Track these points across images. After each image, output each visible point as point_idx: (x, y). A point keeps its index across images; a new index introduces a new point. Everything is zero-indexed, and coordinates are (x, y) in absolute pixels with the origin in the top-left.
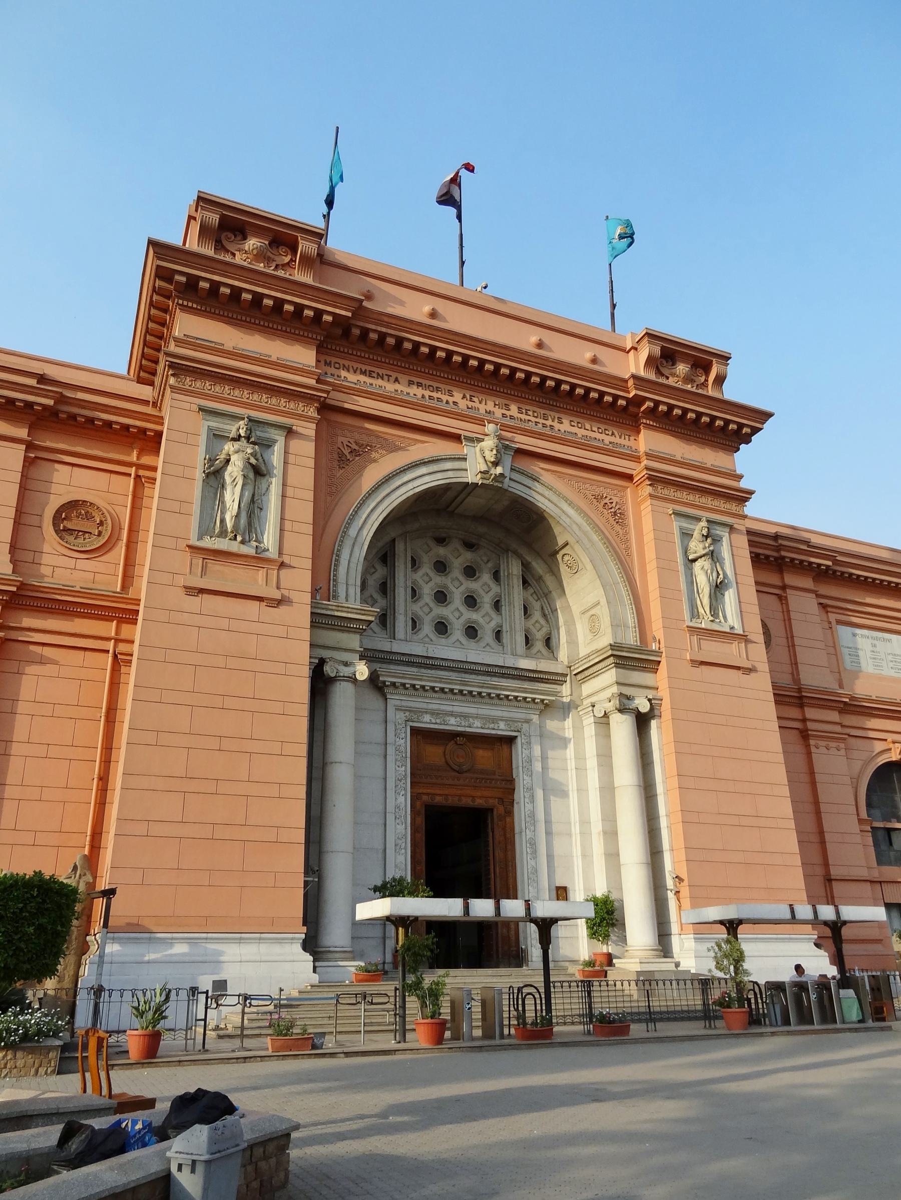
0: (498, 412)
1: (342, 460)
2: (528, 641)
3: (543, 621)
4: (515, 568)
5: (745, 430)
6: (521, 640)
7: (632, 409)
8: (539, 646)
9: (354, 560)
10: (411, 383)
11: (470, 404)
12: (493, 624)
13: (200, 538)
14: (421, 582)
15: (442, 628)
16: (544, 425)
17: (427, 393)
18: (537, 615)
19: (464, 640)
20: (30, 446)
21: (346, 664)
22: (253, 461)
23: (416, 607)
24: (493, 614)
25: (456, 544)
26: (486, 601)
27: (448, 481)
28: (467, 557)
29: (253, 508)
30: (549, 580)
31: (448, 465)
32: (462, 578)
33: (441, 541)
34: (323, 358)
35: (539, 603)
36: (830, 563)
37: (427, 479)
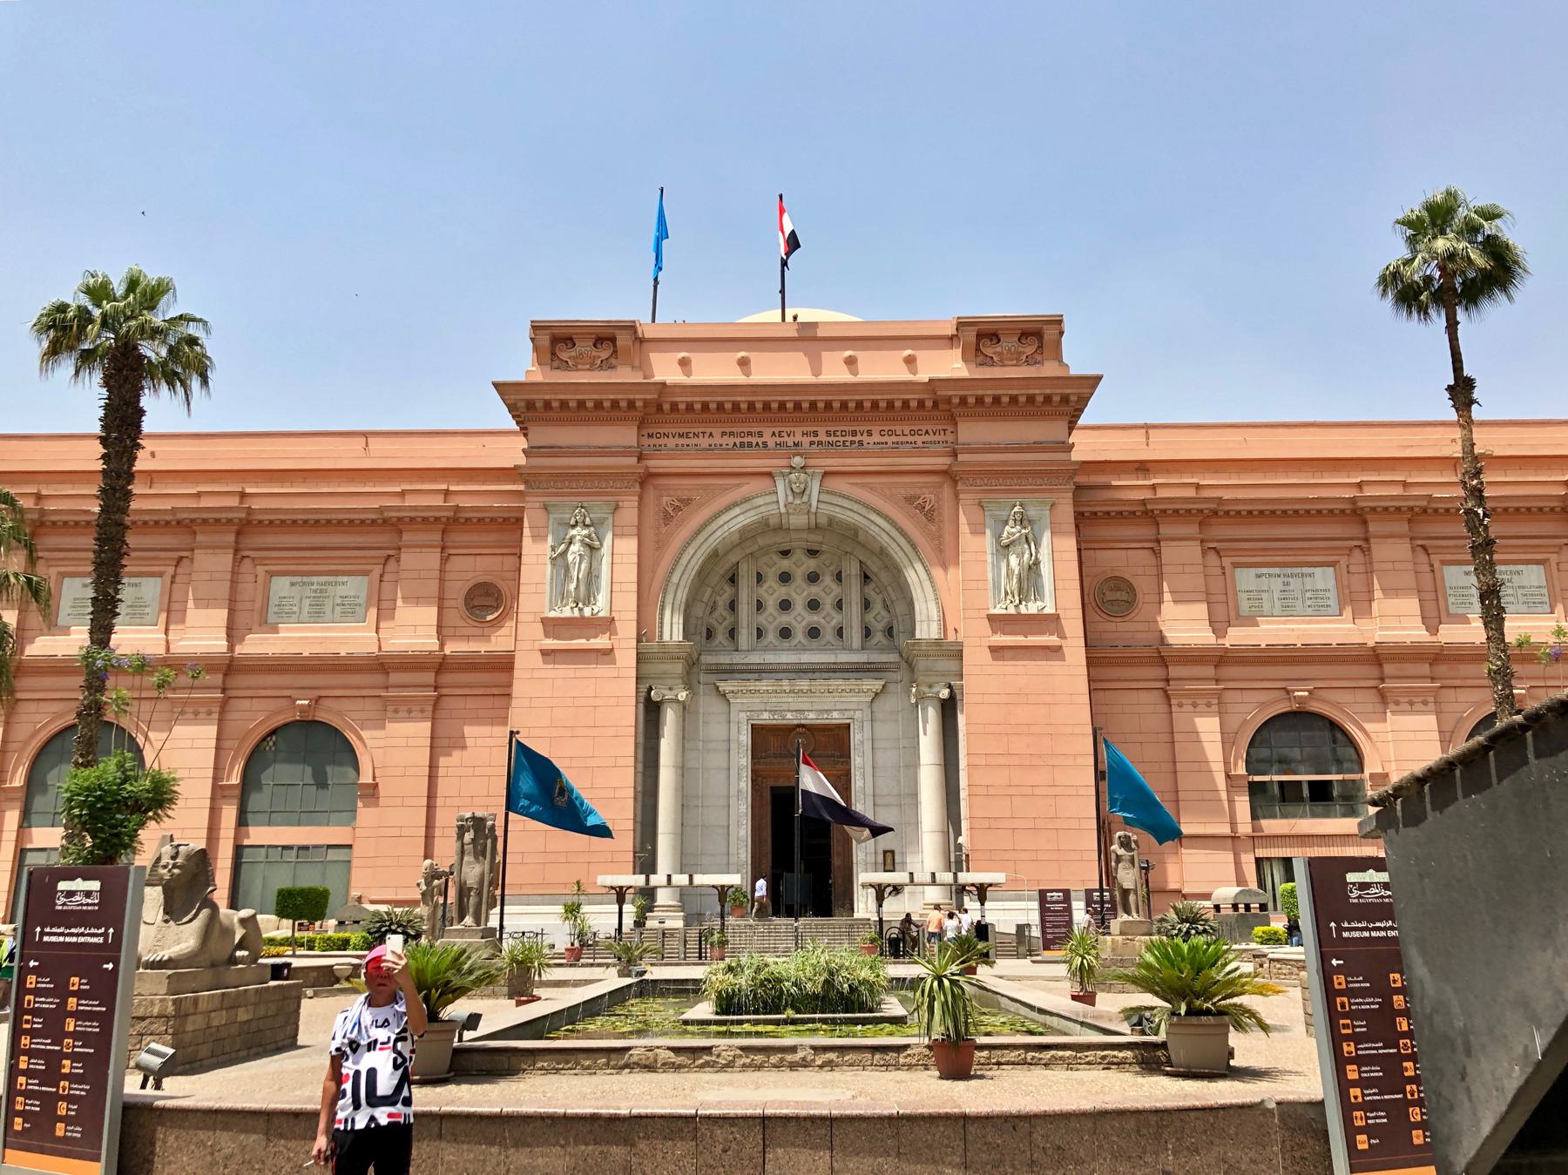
0: (806, 440)
1: (667, 518)
2: (867, 633)
3: (884, 613)
6: (855, 637)
7: (941, 406)
8: (878, 637)
9: (677, 602)
10: (724, 434)
11: (779, 440)
12: (834, 622)
13: (552, 609)
15: (785, 633)
16: (852, 442)
17: (738, 441)
19: (805, 642)
20: (443, 548)
23: (762, 619)
24: (833, 613)
25: (799, 555)
26: (828, 602)
28: (811, 564)
29: (592, 578)
30: (884, 577)
31: (760, 501)
32: (804, 585)
33: (785, 553)
34: (645, 432)
36: (1213, 506)
37: (741, 518)
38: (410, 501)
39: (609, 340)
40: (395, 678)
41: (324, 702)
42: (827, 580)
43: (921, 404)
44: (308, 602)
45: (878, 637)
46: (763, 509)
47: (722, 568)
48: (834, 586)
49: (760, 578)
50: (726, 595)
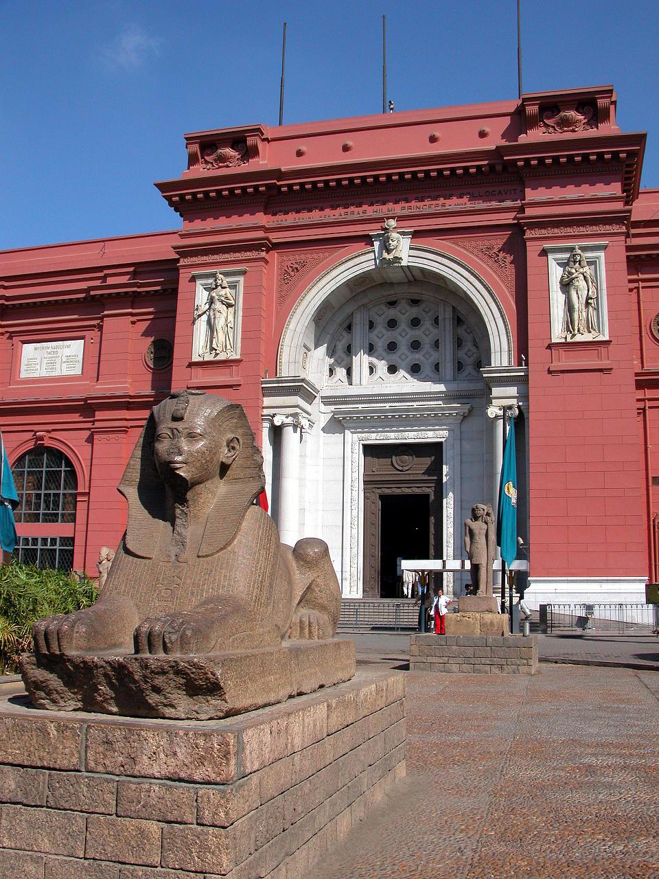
2: (460, 366)
3: (474, 349)
4: (446, 315)
5: (623, 155)
6: (448, 369)
8: (469, 369)
12: (431, 359)
14: (377, 340)
18: (468, 345)
21: (287, 417)
22: (223, 298)
25: (403, 305)
26: (427, 342)
27: (361, 271)
28: (414, 312)
33: (392, 304)
35: (471, 335)
38: (111, 281)
39: (240, 141)
40: (99, 415)
41: (53, 435)
42: (427, 324)
43: (491, 167)
44: (45, 361)
45: (469, 369)
46: (364, 265)
47: (340, 318)
48: (431, 328)
49: (372, 325)
50: (344, 341)
